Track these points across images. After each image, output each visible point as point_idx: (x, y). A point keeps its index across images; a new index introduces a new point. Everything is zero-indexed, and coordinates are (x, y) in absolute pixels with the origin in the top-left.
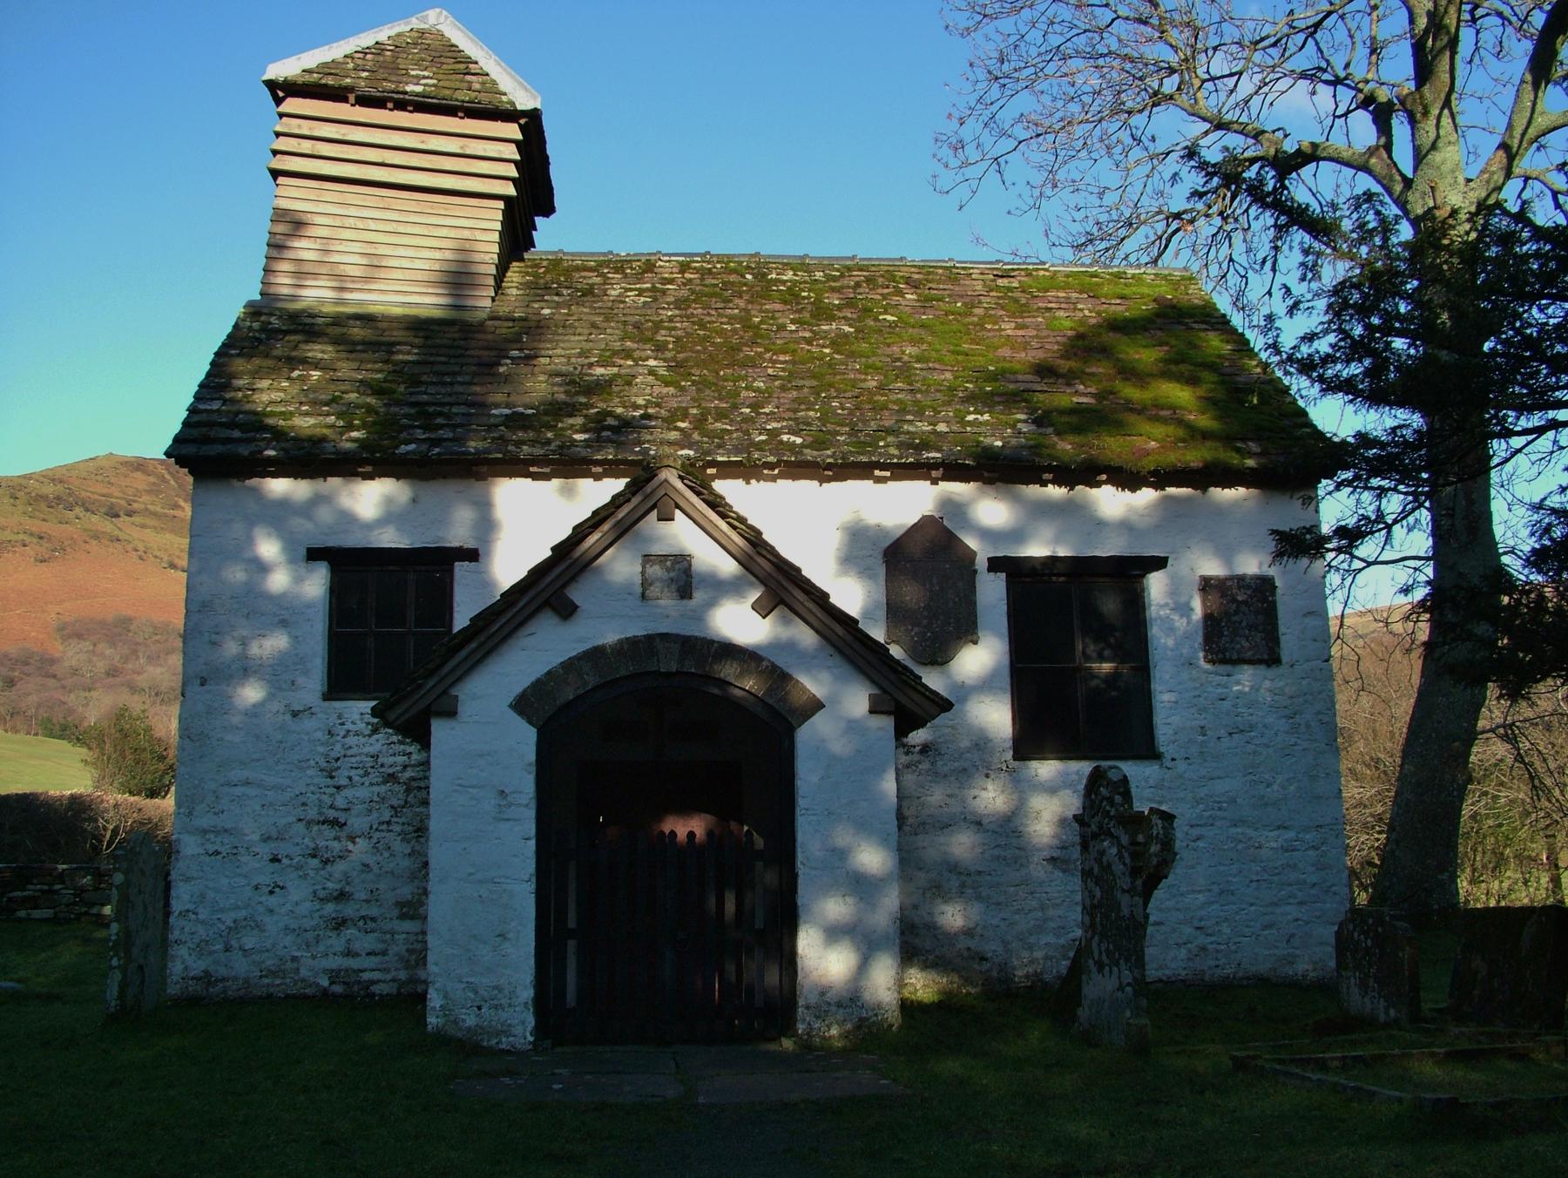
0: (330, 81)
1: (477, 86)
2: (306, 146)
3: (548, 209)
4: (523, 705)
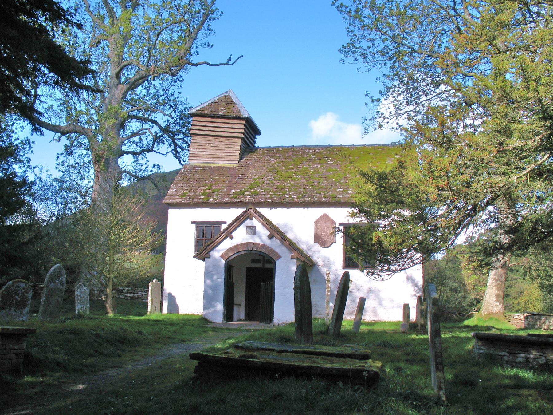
0: (202, 113)
1: (235, 111)
2: (198, 128)
3: (259, 133)
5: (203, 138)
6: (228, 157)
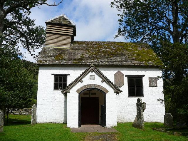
2: (50, 29)
3: (75, 36)
4: (77, 91)
5: (52, 36)
6: (65, 44)
